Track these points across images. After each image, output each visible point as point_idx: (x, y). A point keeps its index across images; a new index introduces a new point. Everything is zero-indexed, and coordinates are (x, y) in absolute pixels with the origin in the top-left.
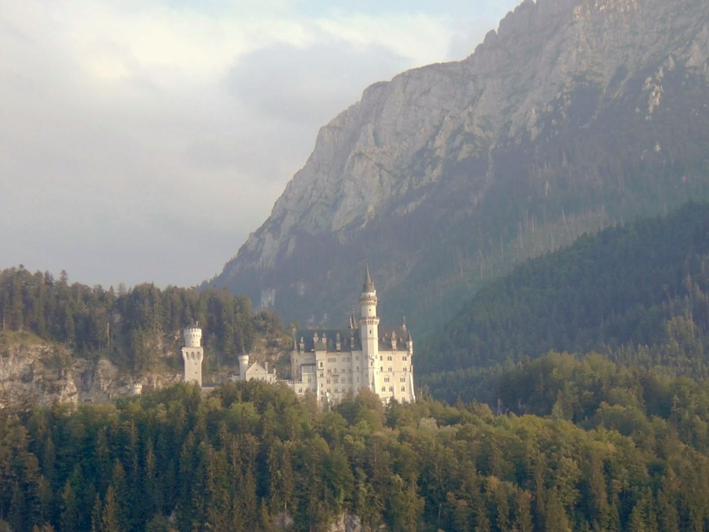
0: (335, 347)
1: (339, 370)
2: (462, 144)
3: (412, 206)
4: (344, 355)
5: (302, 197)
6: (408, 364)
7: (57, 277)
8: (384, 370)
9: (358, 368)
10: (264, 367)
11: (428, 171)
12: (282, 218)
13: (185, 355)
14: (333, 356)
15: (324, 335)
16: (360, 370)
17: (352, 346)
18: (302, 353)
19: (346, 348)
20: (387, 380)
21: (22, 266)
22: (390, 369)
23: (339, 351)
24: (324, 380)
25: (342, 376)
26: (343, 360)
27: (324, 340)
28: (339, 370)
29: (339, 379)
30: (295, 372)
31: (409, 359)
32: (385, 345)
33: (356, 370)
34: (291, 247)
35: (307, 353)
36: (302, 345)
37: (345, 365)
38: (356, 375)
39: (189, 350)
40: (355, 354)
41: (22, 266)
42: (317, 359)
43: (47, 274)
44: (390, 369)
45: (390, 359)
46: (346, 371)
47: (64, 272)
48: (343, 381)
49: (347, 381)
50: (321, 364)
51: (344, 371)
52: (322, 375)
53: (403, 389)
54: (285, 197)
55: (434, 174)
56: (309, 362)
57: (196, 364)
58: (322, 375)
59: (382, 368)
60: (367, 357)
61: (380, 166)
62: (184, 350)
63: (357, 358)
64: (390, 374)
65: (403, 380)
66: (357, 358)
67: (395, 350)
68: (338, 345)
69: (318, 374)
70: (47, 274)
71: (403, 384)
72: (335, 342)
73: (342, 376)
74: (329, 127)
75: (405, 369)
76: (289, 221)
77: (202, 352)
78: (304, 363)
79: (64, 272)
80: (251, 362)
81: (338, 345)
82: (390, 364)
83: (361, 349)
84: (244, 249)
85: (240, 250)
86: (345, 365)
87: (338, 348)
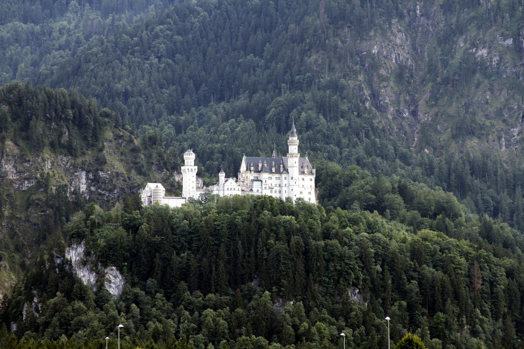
0: (271, 170)
1: (273, 185)
4: (277, 176)
6: (313, 183)
14: (271, 176)
15: (265, 162)
16: (287, 186)
18: (252, 172)
19: (278, 172)
23: (274, 173)
25: (275, 188)
28: (273, 185)
29: (274, 190)
33: (284, 185)
36: (252, 168)
37: (278, 182)
38: (284, 189)
40: (284, 176)
42: (263, 177)
44: (303, 186)
46: (278, 186)
48: (276, 192)
49: (278, 192)
51: (276, 185)
52: (266, 188)
58: (266, 188)
60: (292, 178)
66: (285, 178)
69: (264, 186)
73: (275, 188)
78: (253, 178)
83: (288, 173)
86: (278, 182)
87: (274, 171)
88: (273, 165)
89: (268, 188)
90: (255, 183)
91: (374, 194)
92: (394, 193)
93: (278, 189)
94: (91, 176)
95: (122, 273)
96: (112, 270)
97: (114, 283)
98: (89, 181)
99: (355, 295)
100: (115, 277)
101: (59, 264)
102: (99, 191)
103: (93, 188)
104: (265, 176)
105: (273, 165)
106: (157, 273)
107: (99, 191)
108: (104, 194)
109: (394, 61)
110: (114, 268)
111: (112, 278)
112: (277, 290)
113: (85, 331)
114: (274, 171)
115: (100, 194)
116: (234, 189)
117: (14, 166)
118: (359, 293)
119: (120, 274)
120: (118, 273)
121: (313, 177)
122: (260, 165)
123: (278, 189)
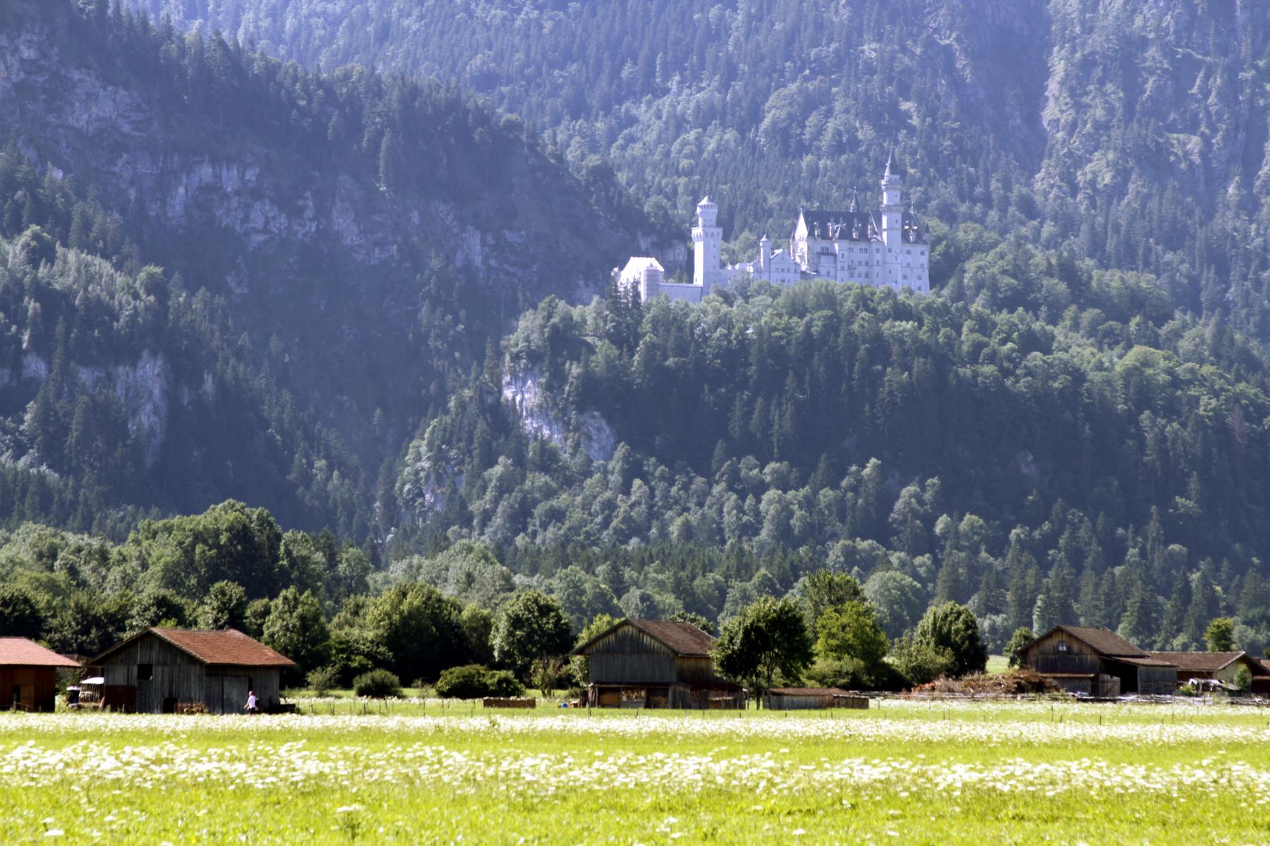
1: (856, 262)
4: (863, 245)
6: (924, 260)
14: (852, 246)
28: (856, 262)
31: (927, 253)
37: (864, 257)
38: (876, 269)
45: (909, 252)
48: (859, 275)
51: (860, 263)
58: (843, 268)
60: (890, 251)
63: (878, 251)
64: (909, 270)
65: (920, 278)
69: (839, 265)
71: (919, 282)
82: (909, 258)
86: (864, 257)
90: (823, 259)
91: (1015, 276)
92: (1052, 276)
93: (863, 269)
94: (490, 239)
95: (610, 422)
96: (593, 417)
97: (599, 441)
98: (487, 249)
100: (599, 430)
101: (491, 406)
102: (506, 266)
103: (493, 262)
107: (506, 266)
108: (514, 274)
109: (990, 21)
110: (596, 413)
111: (594, 433)
113: (559, 529)
115: (507, 273)
116: (789, 270)
117: (354, 220)
119: (608, 424)
120: (604, 423)
123: (863, 269)
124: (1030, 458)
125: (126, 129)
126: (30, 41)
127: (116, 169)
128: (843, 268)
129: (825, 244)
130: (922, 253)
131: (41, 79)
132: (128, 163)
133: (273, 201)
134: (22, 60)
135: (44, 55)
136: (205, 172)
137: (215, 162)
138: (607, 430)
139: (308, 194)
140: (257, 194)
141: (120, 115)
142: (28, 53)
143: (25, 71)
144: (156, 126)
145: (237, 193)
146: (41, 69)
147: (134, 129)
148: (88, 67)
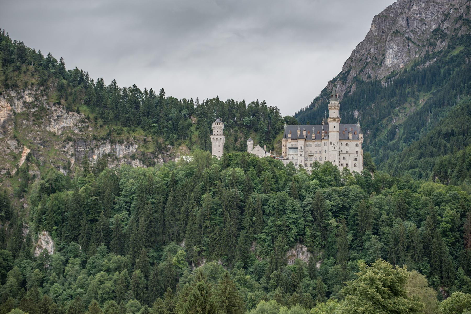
2: (461, 27)
3: (427, 64)
4: (318, 142)
5: (361, 59)
6: (359, 149)
7: (157, 93)
8: (343, 152)
9: (325, 151)
10: (263, 148)
11: (439, 42)
12: (348, 72)
13: (212, 139)
16: (327, 152)
17: (323, 137)
18: (290, 140)
20: (345, 159)
21: (134, 85)
22: (347, 152)
23: (313, 139)
24: (303, 158)
26: (316, 145)
27: (304, 133)
28: (313, 152)
30: (285, 153)
31: (360, 146)
32: (343, 136)
34: (353, 89)
35: (293, 141)
39: (215, 137)
40: (324, 142)
41: (134, 85)
43: (151, 91)
44: (347, 152)
45: (347, 145)
46: (318, 153)
47: (162, 91)
50: (301, 147)
51: (316, 152)
53: (355, 165)
54: (351, 59)
55: (441, 45)
56: (294, 146)
57: (219, 146)
58: (301, 155)
59: (342, 151)
60: (331, 143)
61: (409, 39)
62: (212, 137)
64: (347, 156)
65: (355, 159)
66: (325, 144)
67: (351, 139)
68: (313, 136)
70: (151, 91)
72: (311, 133)
73: (315, 155)
74: (378, 16)
75: (357, 152)
76: (353, 74)
77: (223, 137)
79: (162, 91)
80: (254, 146)
81: (313, 136)
82: (347, 148)
84: (325, 90)
85: (322, 91)
88: (313, 131)
89: (303, 155)
95: (53, 239)
96: (44, 235)
99: (303, 253)
100: (47, 243)
104: (301, 143)
105: (313, 131)
106: (83, 237)
110: (46, 233)
112: (199, 249)
114: (313, 138)
118: (308, 251)
121: (360, 143)
122: (299, 133)
124: (305, 249)
125: (77, 131)
126: (30, 94)
127: (66, 150)
128: (301, 155)
129: (294, 142)
130: (357, 145)
131: (34, 110)
132: (71, 146)
133: (140, 160)
134: (25, 103)
135: (37, 99)
136: (107, 148)
137: (112, 142)
138: (51, 241)
139: (160, 156)
140: (133, 157)
141: (74, 125)
142: (29, 99)
143: (26, 107)
144: (90, 129)
145: (124, 157)
146: (34, 106)
147: (80, 131)
148: (59, 104)
